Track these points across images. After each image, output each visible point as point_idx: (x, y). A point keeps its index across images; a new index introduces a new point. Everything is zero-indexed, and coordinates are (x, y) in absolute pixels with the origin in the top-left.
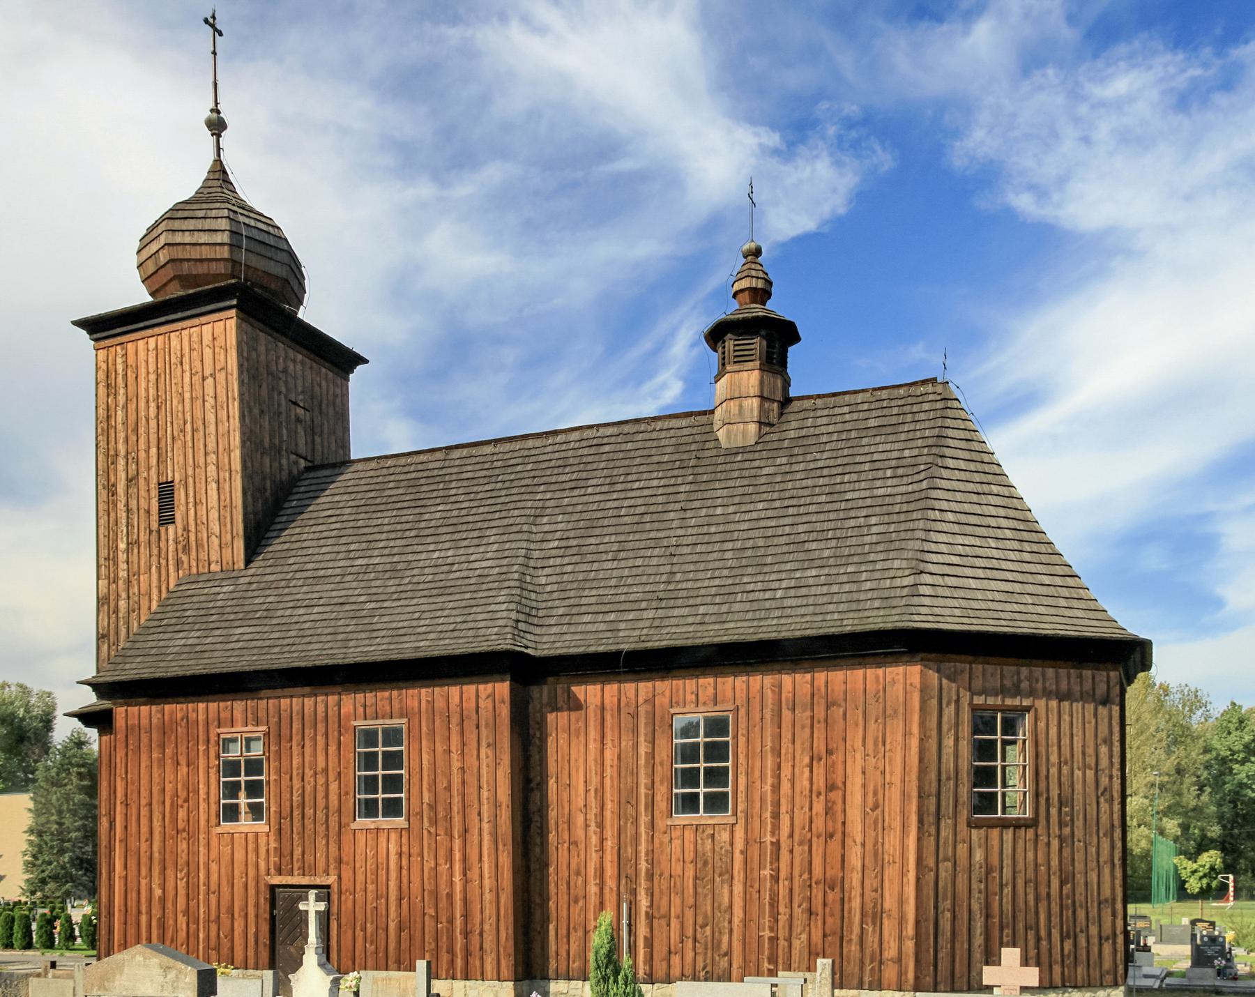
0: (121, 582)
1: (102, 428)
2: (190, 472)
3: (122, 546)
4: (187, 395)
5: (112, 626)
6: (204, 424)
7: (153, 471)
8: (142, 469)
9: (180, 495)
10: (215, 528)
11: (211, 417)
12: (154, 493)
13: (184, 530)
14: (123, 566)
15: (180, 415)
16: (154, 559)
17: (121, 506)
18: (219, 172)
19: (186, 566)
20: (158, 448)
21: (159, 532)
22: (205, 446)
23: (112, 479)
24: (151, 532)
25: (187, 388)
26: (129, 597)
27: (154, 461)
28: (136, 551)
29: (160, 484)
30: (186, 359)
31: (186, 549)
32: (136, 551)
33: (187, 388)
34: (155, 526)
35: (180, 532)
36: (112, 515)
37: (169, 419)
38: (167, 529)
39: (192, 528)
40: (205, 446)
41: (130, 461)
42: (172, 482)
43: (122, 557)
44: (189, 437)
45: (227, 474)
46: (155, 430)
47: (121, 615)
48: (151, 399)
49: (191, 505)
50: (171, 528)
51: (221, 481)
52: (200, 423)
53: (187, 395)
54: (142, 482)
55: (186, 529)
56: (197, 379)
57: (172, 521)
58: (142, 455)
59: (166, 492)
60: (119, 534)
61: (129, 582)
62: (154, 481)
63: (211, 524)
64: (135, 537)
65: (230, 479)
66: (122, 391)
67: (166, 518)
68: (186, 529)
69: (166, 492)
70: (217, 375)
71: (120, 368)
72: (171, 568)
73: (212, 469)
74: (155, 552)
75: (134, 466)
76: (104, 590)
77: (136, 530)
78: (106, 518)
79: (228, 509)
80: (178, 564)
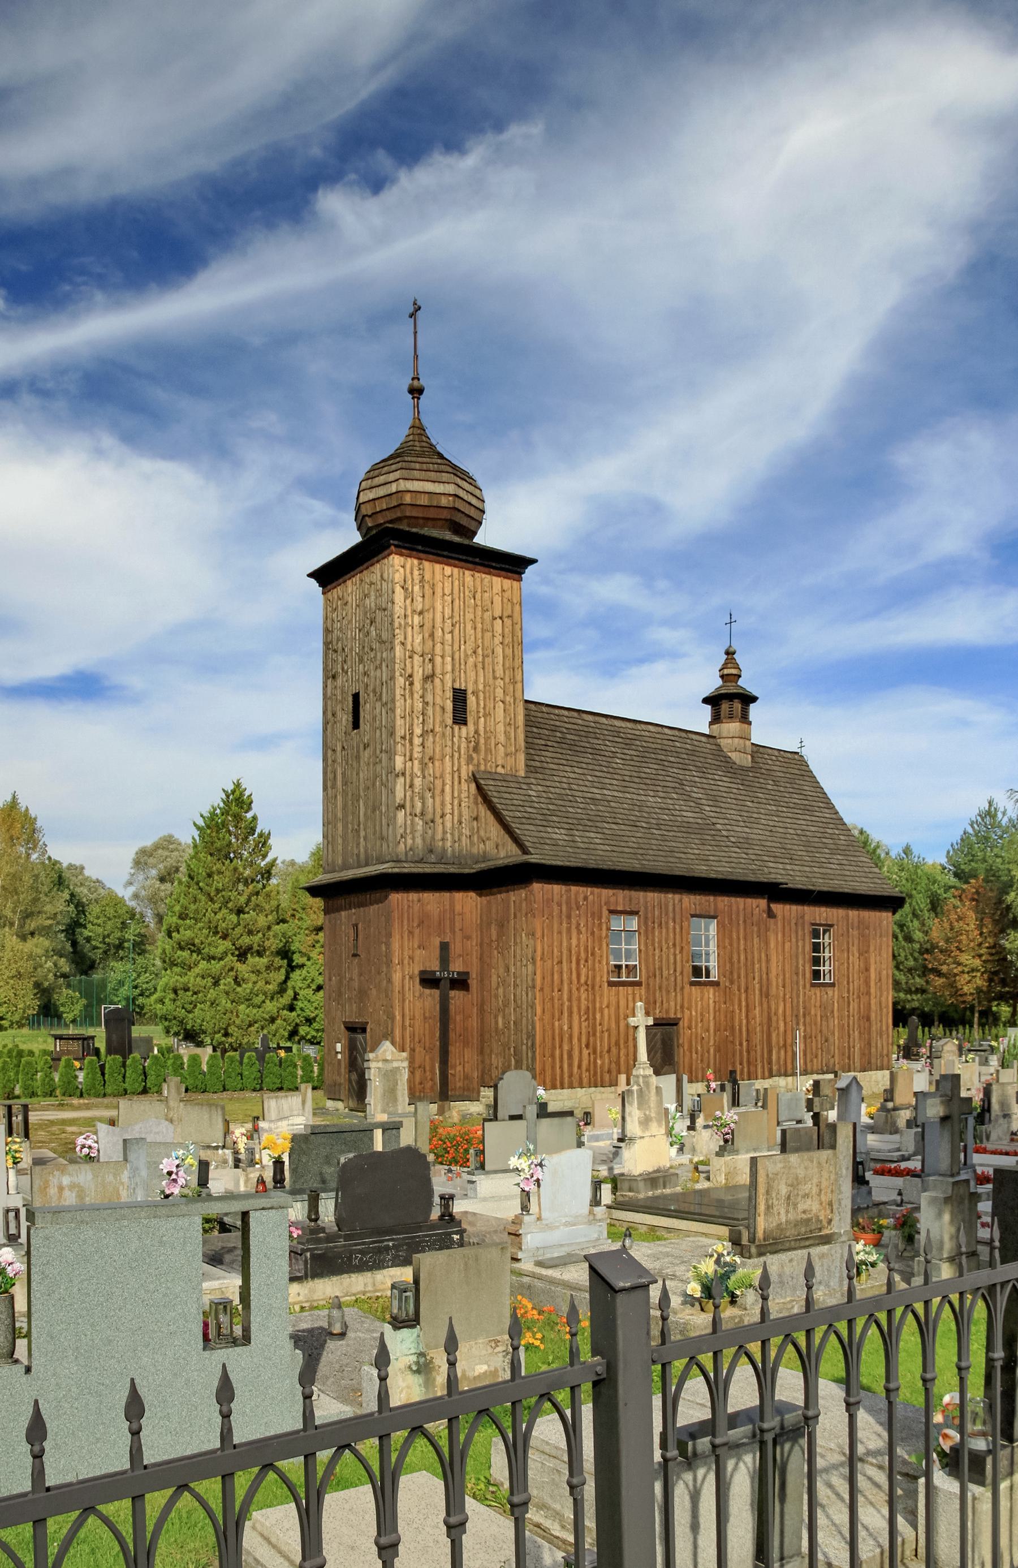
0: (416, 762)
1: (400, 624)
2: (481, 687)
3: (418, 731)
4: (479, 626)
5: (408, 798)
7: (448, 678)
8: (438, 671)
10: (502, 738)
11: (499, 650)
12: (449, 694)
14: (417, 749)
15: (473, 638)
16: (448, 750)
17: (416, 696)
18: (418, 429)
19: (475, 761)
20: (453, 659)
21: (452, 728)
22: (494, 671)
23: (409, 671)
25: (478, 619)
26: (424, 777)
27: (449, 668)
28: (431, 739)
30: (478, 596)
31: (476, 749)
32: (431, 739)
33: (478, 619)
34: (449, 721)
35: (472, 734)
36: (409, 701)
37: (462, 639)
39: (482, 733)
40: (494, 671)
41: (427, 660)
43: (417, 741)
44: (480, 659)
46: (450, 642)
47: (417, 790)
48: (446, 616)
49: (481, 715)
50: (464, 729)
52: (490, 651)
53: (479, 626)
54: (437, 681)
55: (476, 732)
56: (488, 615)
57: (464, 722)
58: (438, 660)
59: (460, 697)
60: (416, 720)
61: (424, 766)
63: (498, 735)
64: (431, 727)
68: (476, 732)
69: (460, 697)
70: (505, 620)
72: (463, 762)
73: (499, 692)
74: (449, 743)
75: (430, 666)
77: (431, 721)
78: (402, 701)
80: (470, 759)
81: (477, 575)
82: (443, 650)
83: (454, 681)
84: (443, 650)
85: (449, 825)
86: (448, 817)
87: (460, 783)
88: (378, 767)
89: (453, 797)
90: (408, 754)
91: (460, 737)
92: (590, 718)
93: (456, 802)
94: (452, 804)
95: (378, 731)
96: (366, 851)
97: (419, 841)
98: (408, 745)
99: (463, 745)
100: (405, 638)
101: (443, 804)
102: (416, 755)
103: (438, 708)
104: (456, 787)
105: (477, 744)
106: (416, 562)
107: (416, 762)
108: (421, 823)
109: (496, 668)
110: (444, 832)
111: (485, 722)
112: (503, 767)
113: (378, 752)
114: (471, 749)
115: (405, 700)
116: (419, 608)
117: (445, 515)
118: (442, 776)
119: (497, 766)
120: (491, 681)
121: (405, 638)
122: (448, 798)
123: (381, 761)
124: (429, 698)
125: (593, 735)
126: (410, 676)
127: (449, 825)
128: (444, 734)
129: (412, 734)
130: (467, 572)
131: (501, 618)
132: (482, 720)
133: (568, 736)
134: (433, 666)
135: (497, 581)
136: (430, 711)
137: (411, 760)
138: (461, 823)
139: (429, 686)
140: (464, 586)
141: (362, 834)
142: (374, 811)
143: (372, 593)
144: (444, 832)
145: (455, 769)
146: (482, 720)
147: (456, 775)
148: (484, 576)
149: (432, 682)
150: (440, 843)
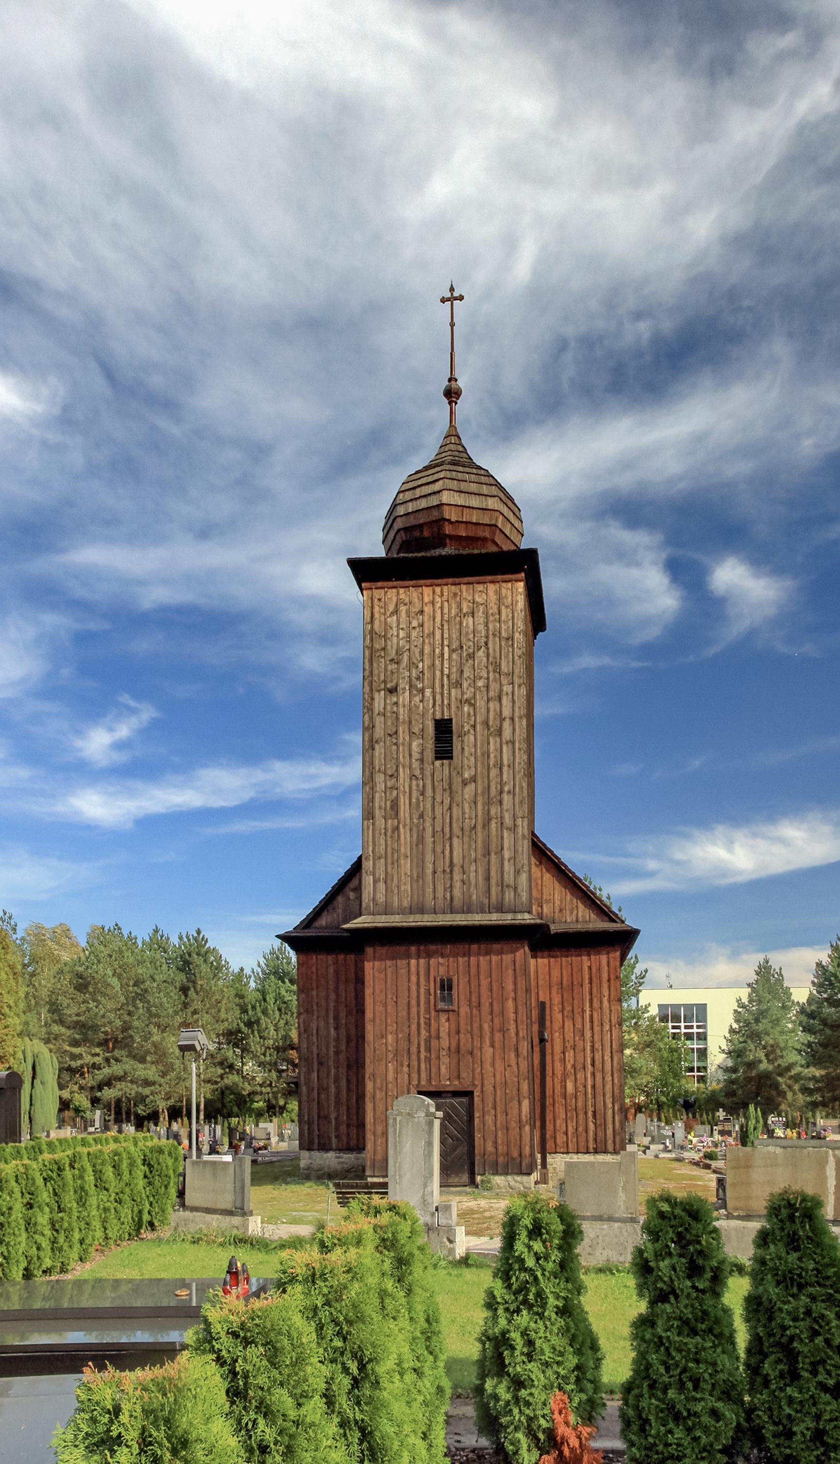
123: (501, 803)
141: (457, 877)
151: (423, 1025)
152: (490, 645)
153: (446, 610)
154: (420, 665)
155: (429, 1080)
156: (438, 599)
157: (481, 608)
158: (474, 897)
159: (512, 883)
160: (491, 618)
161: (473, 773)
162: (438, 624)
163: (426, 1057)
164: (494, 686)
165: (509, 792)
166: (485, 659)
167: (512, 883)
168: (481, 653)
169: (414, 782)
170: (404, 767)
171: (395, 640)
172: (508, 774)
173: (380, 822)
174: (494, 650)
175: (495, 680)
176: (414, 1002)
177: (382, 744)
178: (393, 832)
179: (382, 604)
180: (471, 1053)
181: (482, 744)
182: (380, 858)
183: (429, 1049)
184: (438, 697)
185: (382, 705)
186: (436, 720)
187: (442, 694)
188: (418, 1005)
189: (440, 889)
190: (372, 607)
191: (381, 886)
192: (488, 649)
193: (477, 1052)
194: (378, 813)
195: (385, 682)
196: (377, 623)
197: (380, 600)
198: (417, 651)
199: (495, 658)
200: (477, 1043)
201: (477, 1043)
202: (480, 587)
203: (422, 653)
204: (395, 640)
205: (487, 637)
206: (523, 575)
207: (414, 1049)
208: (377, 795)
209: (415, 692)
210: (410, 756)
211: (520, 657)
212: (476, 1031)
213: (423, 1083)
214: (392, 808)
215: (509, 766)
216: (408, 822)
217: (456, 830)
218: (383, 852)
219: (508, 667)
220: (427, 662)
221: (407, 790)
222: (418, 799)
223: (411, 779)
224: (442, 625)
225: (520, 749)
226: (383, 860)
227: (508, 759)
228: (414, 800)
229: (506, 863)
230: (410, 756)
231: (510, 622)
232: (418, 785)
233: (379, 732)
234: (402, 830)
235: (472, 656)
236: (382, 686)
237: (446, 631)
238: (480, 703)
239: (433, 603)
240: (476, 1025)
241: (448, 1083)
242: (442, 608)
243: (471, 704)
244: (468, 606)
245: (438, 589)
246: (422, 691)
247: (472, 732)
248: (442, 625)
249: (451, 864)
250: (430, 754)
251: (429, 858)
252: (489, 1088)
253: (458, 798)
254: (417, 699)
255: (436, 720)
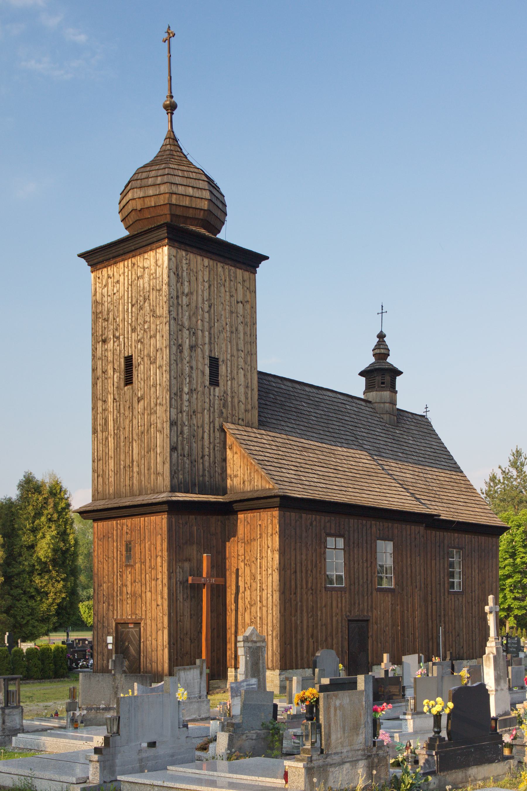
0: (185, 414)
3: (186, 390)
6: (237, 330)
8: (200, 342)
9: (222, 369)
10: (243, 398)
11: (241, 328)
12: (207, 361)
13: (225, 393)
17: (185, 362)
23: (180, 341)
24: (205, 387)
27: (207, 340)
29: (210, 357)
30: (227, 284)
31: (225, 406)
32: (195, 396)
34: (207, 383)
36: (180, 365)
38: (214, 389)
39: (229, 393)
40: (237, 345)
42: (218, 359)
43: (186, 397)
45: (249, 368)
47: (185, 436)
48: (205, 299)
50: (217, 389)
51: (246, 370)
52: (234, 329)
62: (207, 353)
65: (251, 371)
66: (186, 284)
67: (214, 381)
71: (185, 267)
76: (174, 417)
78: (175, 365)
79: (250, 389)
81: (226, 267)
82: (203, 325)
83: (211, 351)
84: (203, 325)
85: (207, 464)
86: (207, 458)
87: (214, 432)
88: (153, 417)
89: (210, 443)
90: (179, 407)
91: (214, 396)
92: (289, 384)
93: (212, 446)
94: (209, 448)
95: (153, 390)
96: (140, 481)
97: (186, 475)
98: (179, 400)
99: (217, 402)
100: (178, 314)
101: (203, 448)
102: (185, 408)
103: (199, 372)
104: (212, 435)
105: (226, 401)
106: (184, 253)
107: (185, 414)
108: (187, 461)
109: (239, 342)
110: (204, 470)
111: (232, 385)
112: (243, 420)
113: (152, 405)
114: (222, 406)
115: (177, 365)
116: (186, 291)
117: (201, 215)
118: (203, 426)
119: (239, 419)
120: (235, 353)
121: (178, 314)
122: (206, 443)
123: (156, 412)
124: (194, 364)
125: (294, 398)
126: (180, 345)
127: (207, 464)
128: (203, 393)
129: (181, 390)
130: (219, 265)
131: (242, 302)
132: (229, 382)
133: (278, 398)
134: (197, 339)
135: (239, 272)
136: (194, 376)
137: (181, 412)
138: (215, 463)
139: (193, 354)
140: (217, 275)
141: (136, 469)
142: (149, 451)
143: (146, 276)
144: (204, 470)
145: (211, 420)
146: (229, 382)
147: (212, 425)
148: (230, 268)
149: (195, 351)
150: (201, 479)
151: (119, 577)
152: (151, 297)
153: (130, 278)
154: (118, 320)
155: (122, 615)
156: (126, 270)
157: (146, 270)
158: (143, 483)
159: (161, 472)
160: (152, 277)
161: (142, 393)
162: (126, 289)
163: (120, 599)
164: (153, 326)
165: (160, 404)
166: (148, 308)
167: (161, 472)
168: (146, 304)
169: (115, 404)
170: (110, 393)
171: (106, 304)
172: (159, 390)
173: (100, 435)
174: (153, 301)
175: (153, 323)
176: (115, 561)
177: (100, 379)
178: (106, 441)
179: (100, 281)
180: (141, 596)
181: (147, 371)
182: (100, 460)
183: (121, 594)
184: (126, 340)
185: (100, 352)
186: (125, 357)
187: (128, 338)
188: (117, 563)
189: (127, 478)
190: (96, 284)
191: (100, 480)
192: (149, 300)
193: (143, 595)
194: (99, 428)
195: (102, 335)
196: (98, 294)
197: (99, 278)
198: (116, 310)
199: (153, 306)
200: (144, 589)
201: (144, 589)
202: (146, 256)
203: (118, 311)
204: (106, 304)
205: (149, 292)
206: (166, 241)
207: (115, 594)
208: (98, 415)
209: (115, 340)
210: (113, 385)
211: (165, 302)
212: (143, 581)
213: (119, 617)
214: (105, 424)
215: (160, 385)
216: (112, 433)
217: (135, 437)
218: (101, 456)
219: (159, 311)
220: (121, 317)
221: (112, 410)
222: (117, 416)
223: (114, 402)
224: (128, 288)
225: (165, 371)
226: (101, 461)
227: (160, 379)
228: (115, 417)
229: (158, 456)
230: (113, 385)
231: (161, 278)
232: (117, 406)
233: (99, 372)
234: (109, 439)
235: (141, 308)
236: (100, 339)
237: (130, 292)
238: (146, 341)
239: (124, 273)
240: (143, 576)
241: (130, 617)
242: (128, 276)
243: (142, 343)
244: (140, 271)
245: (126, 263)
246: (118, 338)
247: (142, 363)
248: (128, 288)
249: (133, 461)
250: (122, 383)
251: (122, 457)
252: (148, 622)
253: (135, 413)
254: (116, 344)
255: (125, 357)
